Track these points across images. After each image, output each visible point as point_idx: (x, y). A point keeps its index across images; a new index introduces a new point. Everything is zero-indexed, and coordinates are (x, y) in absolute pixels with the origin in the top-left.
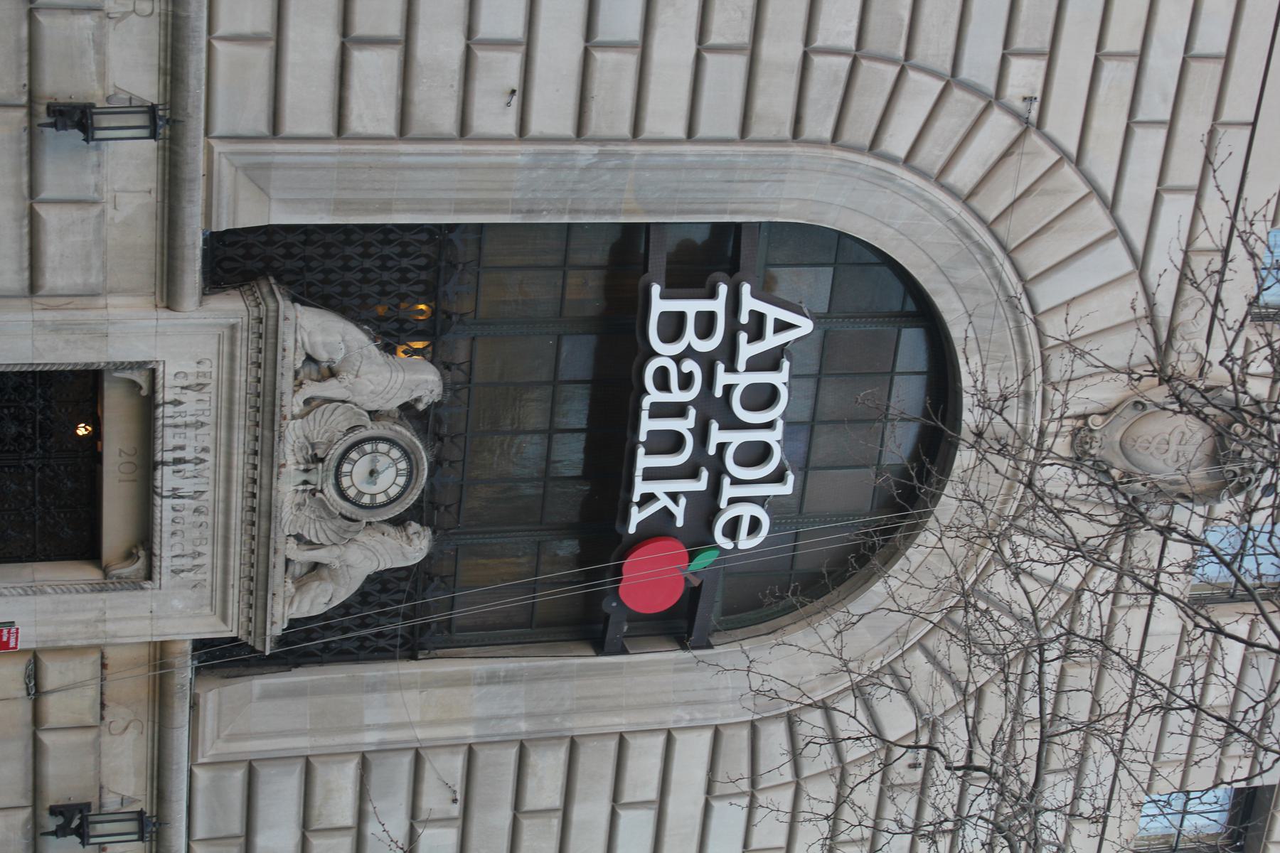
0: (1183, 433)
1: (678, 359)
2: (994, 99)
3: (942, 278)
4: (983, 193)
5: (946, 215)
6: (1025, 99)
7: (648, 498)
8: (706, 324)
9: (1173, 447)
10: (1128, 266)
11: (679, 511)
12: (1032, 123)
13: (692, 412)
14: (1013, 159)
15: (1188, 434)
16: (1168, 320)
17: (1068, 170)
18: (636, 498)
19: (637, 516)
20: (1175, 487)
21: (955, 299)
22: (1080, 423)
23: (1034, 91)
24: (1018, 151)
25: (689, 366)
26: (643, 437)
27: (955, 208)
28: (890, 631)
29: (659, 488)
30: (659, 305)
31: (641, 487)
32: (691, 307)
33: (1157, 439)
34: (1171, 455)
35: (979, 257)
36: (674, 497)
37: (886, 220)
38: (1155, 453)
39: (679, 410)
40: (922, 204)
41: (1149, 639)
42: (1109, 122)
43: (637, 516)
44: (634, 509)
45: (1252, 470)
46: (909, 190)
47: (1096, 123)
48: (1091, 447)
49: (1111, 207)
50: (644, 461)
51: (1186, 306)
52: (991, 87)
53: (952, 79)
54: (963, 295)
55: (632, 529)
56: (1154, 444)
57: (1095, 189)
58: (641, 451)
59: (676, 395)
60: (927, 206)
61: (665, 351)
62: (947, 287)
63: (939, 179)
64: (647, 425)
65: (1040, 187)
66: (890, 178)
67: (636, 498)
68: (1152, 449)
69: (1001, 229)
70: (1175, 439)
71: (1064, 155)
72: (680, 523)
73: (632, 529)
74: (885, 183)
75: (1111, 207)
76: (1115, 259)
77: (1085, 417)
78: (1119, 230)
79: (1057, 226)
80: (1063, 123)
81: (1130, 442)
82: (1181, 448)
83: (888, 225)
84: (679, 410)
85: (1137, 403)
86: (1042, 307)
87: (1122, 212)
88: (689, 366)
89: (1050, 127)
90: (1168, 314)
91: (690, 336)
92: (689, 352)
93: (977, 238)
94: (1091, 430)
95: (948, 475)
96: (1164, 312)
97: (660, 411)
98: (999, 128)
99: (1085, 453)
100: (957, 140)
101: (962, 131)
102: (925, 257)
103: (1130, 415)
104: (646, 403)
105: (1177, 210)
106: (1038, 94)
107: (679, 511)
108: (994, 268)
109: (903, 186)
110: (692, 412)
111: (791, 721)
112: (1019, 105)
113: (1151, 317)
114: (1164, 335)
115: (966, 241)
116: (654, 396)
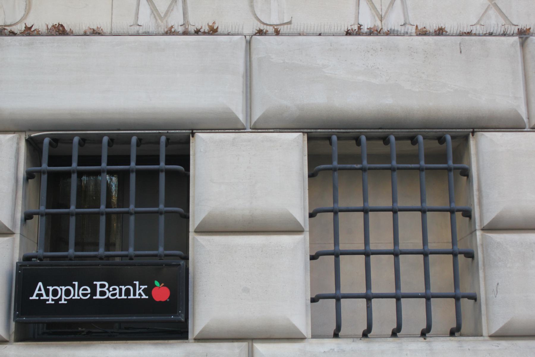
1: (110, 291)
7: (140, 295)
8: (102, 286)
11: (143, 287)
13: (120, 287)
18: (139, 297)
19: (144, 297)
25: (111, 289)
26: (126, 297)
29: (138, 292)
30: (98, 297)
31: (137, 297)
32: (99, 289)
36: (140, 289)
39: (121, 290)
43: (144, 297)
44: (142, 297)
50: (132, 297)
55: (147, 297)
58: (129, 297)
59: (117, 291)
61: (108, 295)
64: (123, 297)
67: (139, 297)
72: (146, 287)
73: (147, 297)
84: (121, 290)
88: (111, 289)
91: (105, 289)
92: (108, 289)
97: (120, 295)
104: (119, 298)
107: (143, 287)
110: (120, 287)
116: (117, 296)
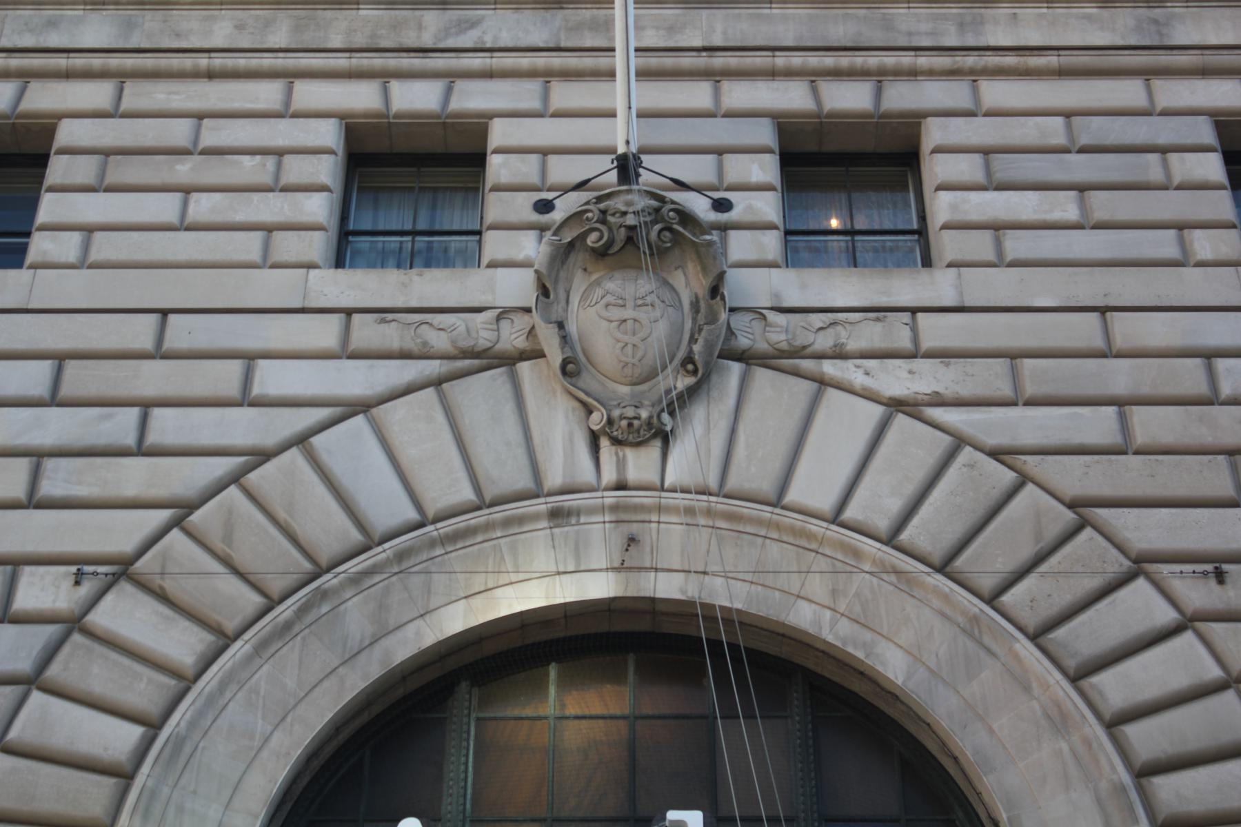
0: (607, 305)
2: (74, 623)
3: (363, 657)
4: (215, 617)
5: (249, 659)
6: (77, 583)
9: (629, 313)
10: (359, 421)
12: (122, 570)
14: (169, 585)
15: (609, 298)
16: (445, 362)
17: (196, 517)
20: (703, 305)
21: (399, 634)
22: (604, 443)
23: (67, 575)
24: (157, 581)
27: (238, 649)
28: (971, 645)
33: (619, 335)
34: (642, 315)
35: (324, 609)
37: (257, 744)
38: (641, 335)
40: (228, 695)
41: (968, 304)
42: (133, 476)
45: (657, 210)
46: (200, 714)
47: (130, 491)
48: (638, 418)
49: (262, 456)
51: (425, 344)
52: (49, 632)
53: (33, 681)
54: (392, 623)
56: (626, 338)
57: (235, 478)
60: (233, 687)
62: (378, 649)
63: (186, 681)
65: (219, 546)
66: (178, 743)
68: (635, 340)
69: (276, 586)
70: (617, 313)
71: (177, 523)
74: (187, 749)
75: (262, 456)
76: (348, 445)
77: (594, 440)
78: (301, 440)
79: (282, 515)
80: (119, 533)
81: (628, 371)
82: (630, 304)
83: (267, 740)
85: (564, 372)
86: (412, 515)
87: (270, 440)
89: (127, 545)
90: (438, 362)
93: (288, 614)
94: (610, 422)
95: (691, 603)
96: (433, 368)
98: (124, 613)
99: (649, 424)
100: (126, 661)
101: (114, 656)
102: (326, 684)
103: (587, 380)
105: (273, 378)
106: (74, 569)
108: (342, 586)
109: (193, 724)
111: (1145, 772)
112: (86, 589)
113: (437, 383)
114: (476, 362)
115: (296, 629)
